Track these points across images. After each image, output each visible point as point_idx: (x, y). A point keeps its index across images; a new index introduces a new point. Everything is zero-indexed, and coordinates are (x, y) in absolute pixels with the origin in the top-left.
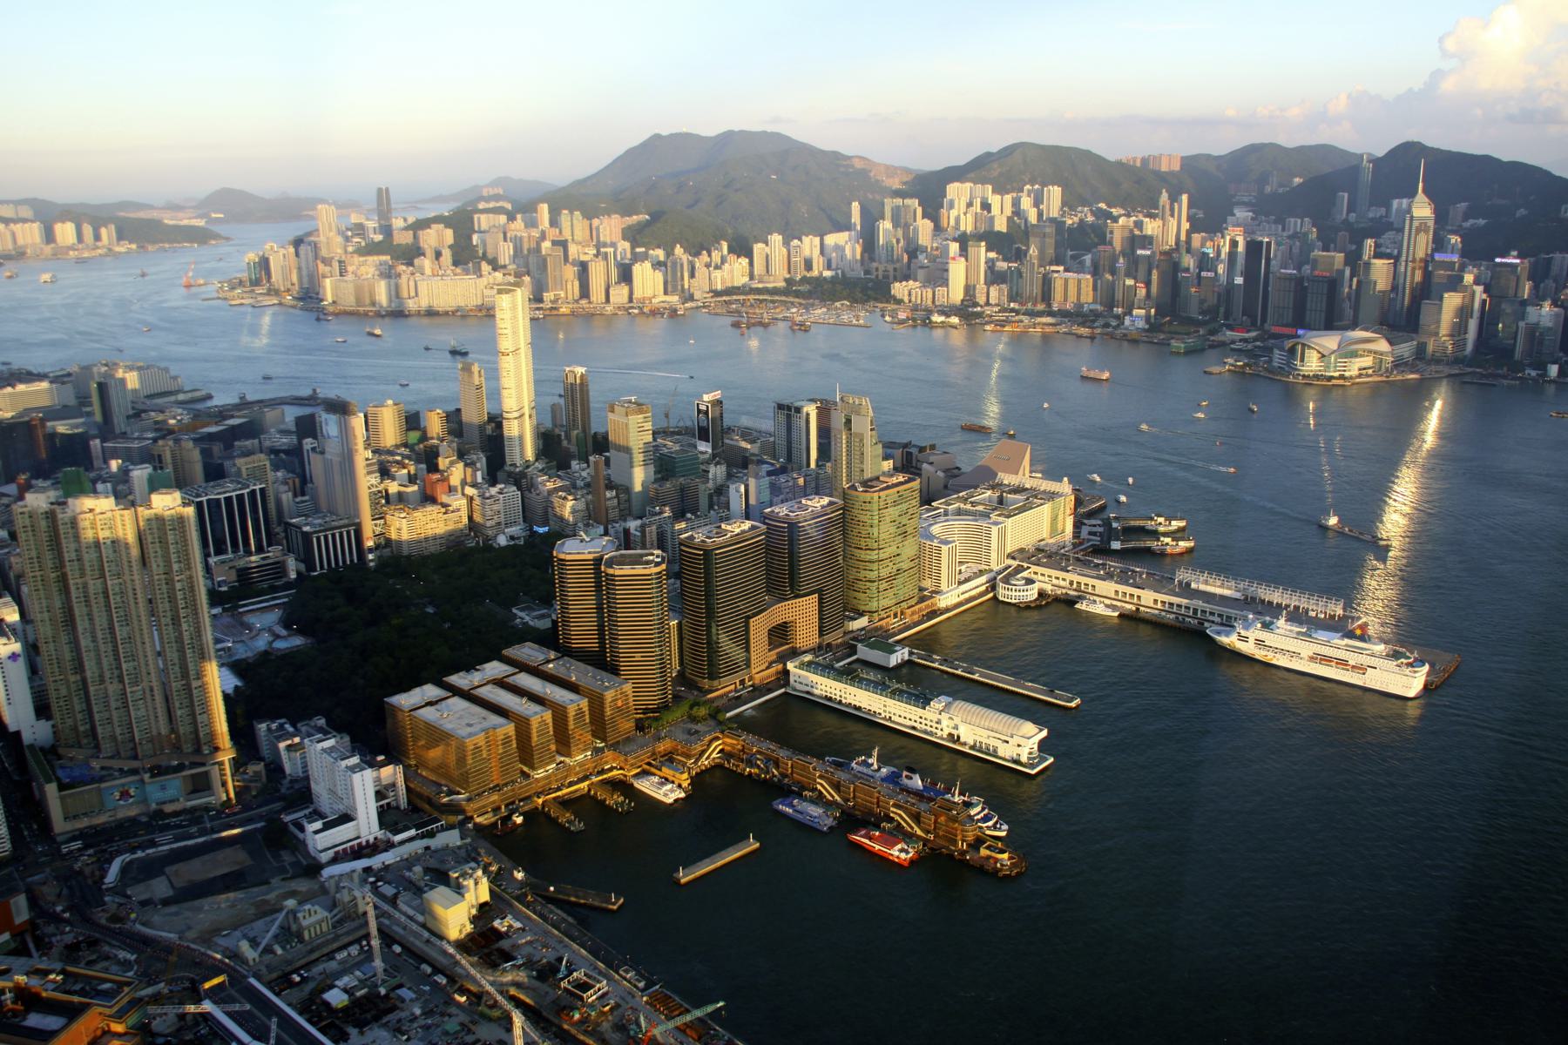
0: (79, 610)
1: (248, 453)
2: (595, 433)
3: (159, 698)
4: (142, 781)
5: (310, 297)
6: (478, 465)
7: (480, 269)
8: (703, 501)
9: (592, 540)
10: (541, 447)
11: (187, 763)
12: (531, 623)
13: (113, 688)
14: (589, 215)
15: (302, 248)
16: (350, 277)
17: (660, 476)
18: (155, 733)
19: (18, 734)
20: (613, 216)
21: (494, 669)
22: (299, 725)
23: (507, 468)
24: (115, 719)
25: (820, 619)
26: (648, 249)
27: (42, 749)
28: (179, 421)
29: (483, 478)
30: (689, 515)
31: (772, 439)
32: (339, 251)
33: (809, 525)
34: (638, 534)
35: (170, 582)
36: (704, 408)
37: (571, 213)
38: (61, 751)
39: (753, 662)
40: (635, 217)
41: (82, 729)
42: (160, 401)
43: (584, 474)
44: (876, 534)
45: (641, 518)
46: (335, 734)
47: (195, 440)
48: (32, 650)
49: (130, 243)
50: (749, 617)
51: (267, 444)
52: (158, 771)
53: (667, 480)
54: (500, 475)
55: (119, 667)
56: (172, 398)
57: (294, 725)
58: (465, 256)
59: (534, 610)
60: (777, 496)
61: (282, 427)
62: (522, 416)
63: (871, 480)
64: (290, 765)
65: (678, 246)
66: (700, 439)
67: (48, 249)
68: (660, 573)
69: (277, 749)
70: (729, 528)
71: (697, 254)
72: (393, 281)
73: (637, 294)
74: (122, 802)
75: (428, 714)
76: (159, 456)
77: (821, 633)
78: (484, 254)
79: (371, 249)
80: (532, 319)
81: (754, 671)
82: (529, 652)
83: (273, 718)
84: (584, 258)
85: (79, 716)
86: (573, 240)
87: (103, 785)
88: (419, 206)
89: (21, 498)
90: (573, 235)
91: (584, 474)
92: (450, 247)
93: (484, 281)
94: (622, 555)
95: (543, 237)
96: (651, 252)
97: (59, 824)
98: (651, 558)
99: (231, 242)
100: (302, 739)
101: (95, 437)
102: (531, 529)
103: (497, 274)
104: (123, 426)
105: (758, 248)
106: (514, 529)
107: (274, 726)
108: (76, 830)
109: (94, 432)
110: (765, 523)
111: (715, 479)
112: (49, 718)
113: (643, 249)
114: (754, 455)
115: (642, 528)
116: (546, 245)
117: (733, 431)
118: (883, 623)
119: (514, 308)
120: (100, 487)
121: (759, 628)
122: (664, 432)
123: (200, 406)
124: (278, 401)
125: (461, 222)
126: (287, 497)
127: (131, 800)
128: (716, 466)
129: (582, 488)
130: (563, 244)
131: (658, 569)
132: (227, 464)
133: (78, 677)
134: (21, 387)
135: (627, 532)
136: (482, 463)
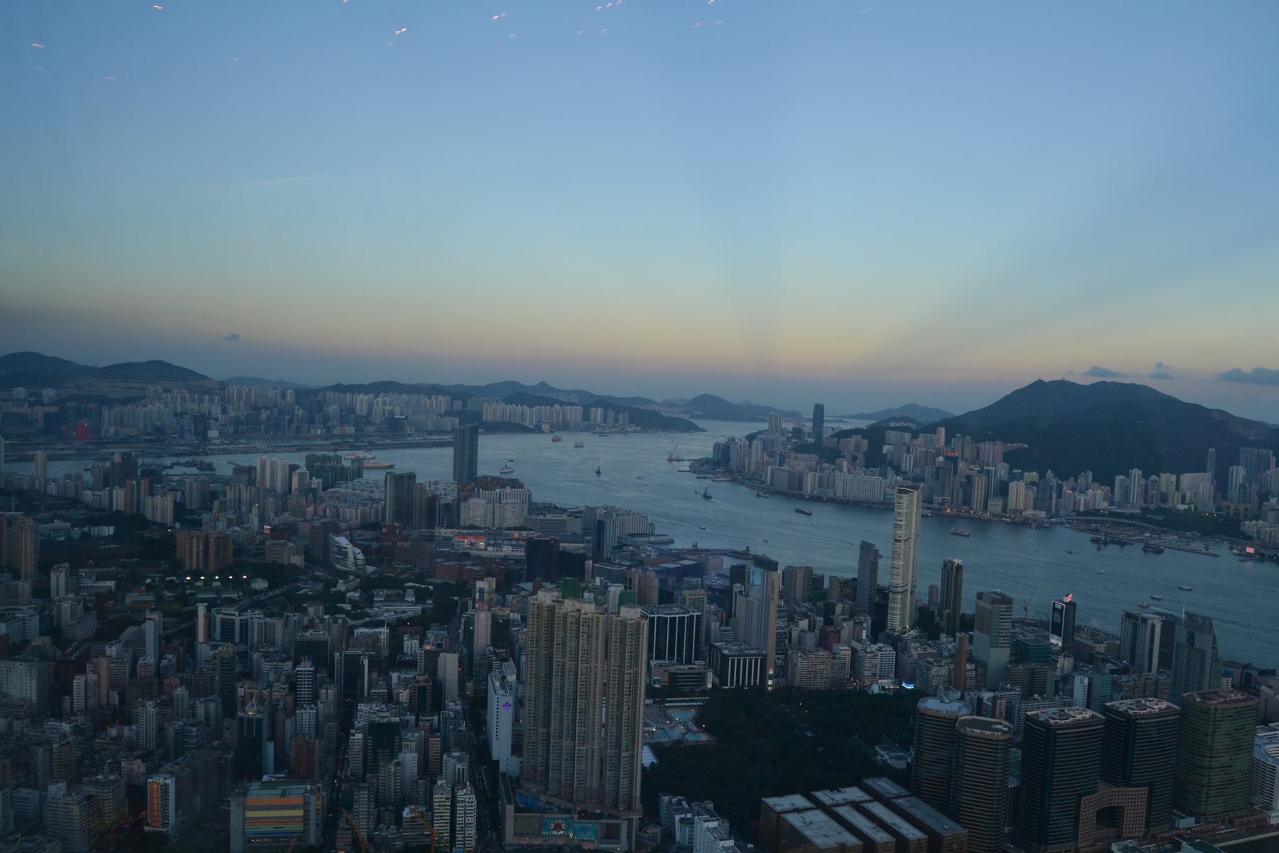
0: (556, 681)
1: (694, 587)
2: (963, 614)
3: (596, 759)
4: (572, 818)
5: (755, 479)
6: (865, 625)
7: (885, 474)
8: (1050, 687)
9: (951, 702)
10: (917, 618)
11: (606, 814)
12: (889, 762)
13: (566, 743)
14: (978, 438)
15: (755, 443)
16: (786, 467)
17: (1013, 658)
18: (588, 785)
19: (498, 762)
20: (997, 442)
21: (854, 793)
22: (693, 804)
23: (887, 631)
24: (563, 769)
25: (1149, 810)
26: (1024, 471)
27: (510, 777)
28: (650, 555)
29: (867, 636)
30: (1036, 696)
31: (1118, 642)
32: (781, 447)
33: (1146, 723)
34: (990, 704)
35: (621, 673)
36: (1059, 606)
37: (963, 436)
38: (522, 782)
39: (1080, 837)
40: (1015, 444)
41: (539, 769)
42: (636, 539)
43: (950, 646)
44: (1209, 744)
45: (994, 691)
46: (718, 817)
47: (657, 572)
48: (519, 703)
50: (1080, 796)
51: (707, 582)
52: (585, 815)
53: (1020, 663)
54: (881, 636)
55: (574, 730)
56: (646, 539)
57: (689, 804)
58: (875, 460)
59: (894, 751)
60: (1118, 693)
61: (721, 572)
62: (906, 591)
63: (1209, 693)
64: (680, 834)
65: (1050, 471)
66: (1053, 632)
68: (1006, 740)
69: (674, 819)
70: (1071, 713)
71: (1067, 479)
72: (818, 474)
73: (1011, 505)
74: (554, 832)
75: (794, 819)
76: (630, 579)
77: (1148, 823)
78: (891, 461)
79: (802, 448)
80: (923, 516)
81: (1079, 845)
82: (885, 785)
83: (675, 795)
84: (970, 473)
85: (540, 759)
86: (962, 457)
87: (545, 816)
88: (844, 419)
89: (534, 592)
90: (962, 454)
91: (950, 646)
92: (864, 453)
93: (888, 481)
94: (974, 719)
95: (938, 454)
96: (1026, 474)
97: (510, 837)
98: (999, 726)
99: (705, 433)
100: (693, 816)
101: (590, 558)
102: (900, 684)
103: (898, 478)
104: (609, 553)
105: (1119, 478)
106: (886, 681)
107: (674, 800)
108: (520, 845)
109: (589, 554)
110: (1104, 714)
111: (1062, 669)
112: (520, 756)
113: (1019, 471)
114: (1100, 653)
115: (994, 699)
116: (941, 459)
117: (1083, 630)
118: (1211, 826)
119: (911, 504)
120: (586, 595)
121: (1089, 808)
122: (1021, 622)
123: (664, 547)
124: (720, 552)
125: (875, 435)
126: (715, 625)
127: (562, 832)
128: (1064, 657)
129: (946, 658)
130: (954, 460)
131: (1005, 737)
132: (676, 593)
133: (545, 731)
134: (549, 516)
135: (980, 700)
136: (867, 623)
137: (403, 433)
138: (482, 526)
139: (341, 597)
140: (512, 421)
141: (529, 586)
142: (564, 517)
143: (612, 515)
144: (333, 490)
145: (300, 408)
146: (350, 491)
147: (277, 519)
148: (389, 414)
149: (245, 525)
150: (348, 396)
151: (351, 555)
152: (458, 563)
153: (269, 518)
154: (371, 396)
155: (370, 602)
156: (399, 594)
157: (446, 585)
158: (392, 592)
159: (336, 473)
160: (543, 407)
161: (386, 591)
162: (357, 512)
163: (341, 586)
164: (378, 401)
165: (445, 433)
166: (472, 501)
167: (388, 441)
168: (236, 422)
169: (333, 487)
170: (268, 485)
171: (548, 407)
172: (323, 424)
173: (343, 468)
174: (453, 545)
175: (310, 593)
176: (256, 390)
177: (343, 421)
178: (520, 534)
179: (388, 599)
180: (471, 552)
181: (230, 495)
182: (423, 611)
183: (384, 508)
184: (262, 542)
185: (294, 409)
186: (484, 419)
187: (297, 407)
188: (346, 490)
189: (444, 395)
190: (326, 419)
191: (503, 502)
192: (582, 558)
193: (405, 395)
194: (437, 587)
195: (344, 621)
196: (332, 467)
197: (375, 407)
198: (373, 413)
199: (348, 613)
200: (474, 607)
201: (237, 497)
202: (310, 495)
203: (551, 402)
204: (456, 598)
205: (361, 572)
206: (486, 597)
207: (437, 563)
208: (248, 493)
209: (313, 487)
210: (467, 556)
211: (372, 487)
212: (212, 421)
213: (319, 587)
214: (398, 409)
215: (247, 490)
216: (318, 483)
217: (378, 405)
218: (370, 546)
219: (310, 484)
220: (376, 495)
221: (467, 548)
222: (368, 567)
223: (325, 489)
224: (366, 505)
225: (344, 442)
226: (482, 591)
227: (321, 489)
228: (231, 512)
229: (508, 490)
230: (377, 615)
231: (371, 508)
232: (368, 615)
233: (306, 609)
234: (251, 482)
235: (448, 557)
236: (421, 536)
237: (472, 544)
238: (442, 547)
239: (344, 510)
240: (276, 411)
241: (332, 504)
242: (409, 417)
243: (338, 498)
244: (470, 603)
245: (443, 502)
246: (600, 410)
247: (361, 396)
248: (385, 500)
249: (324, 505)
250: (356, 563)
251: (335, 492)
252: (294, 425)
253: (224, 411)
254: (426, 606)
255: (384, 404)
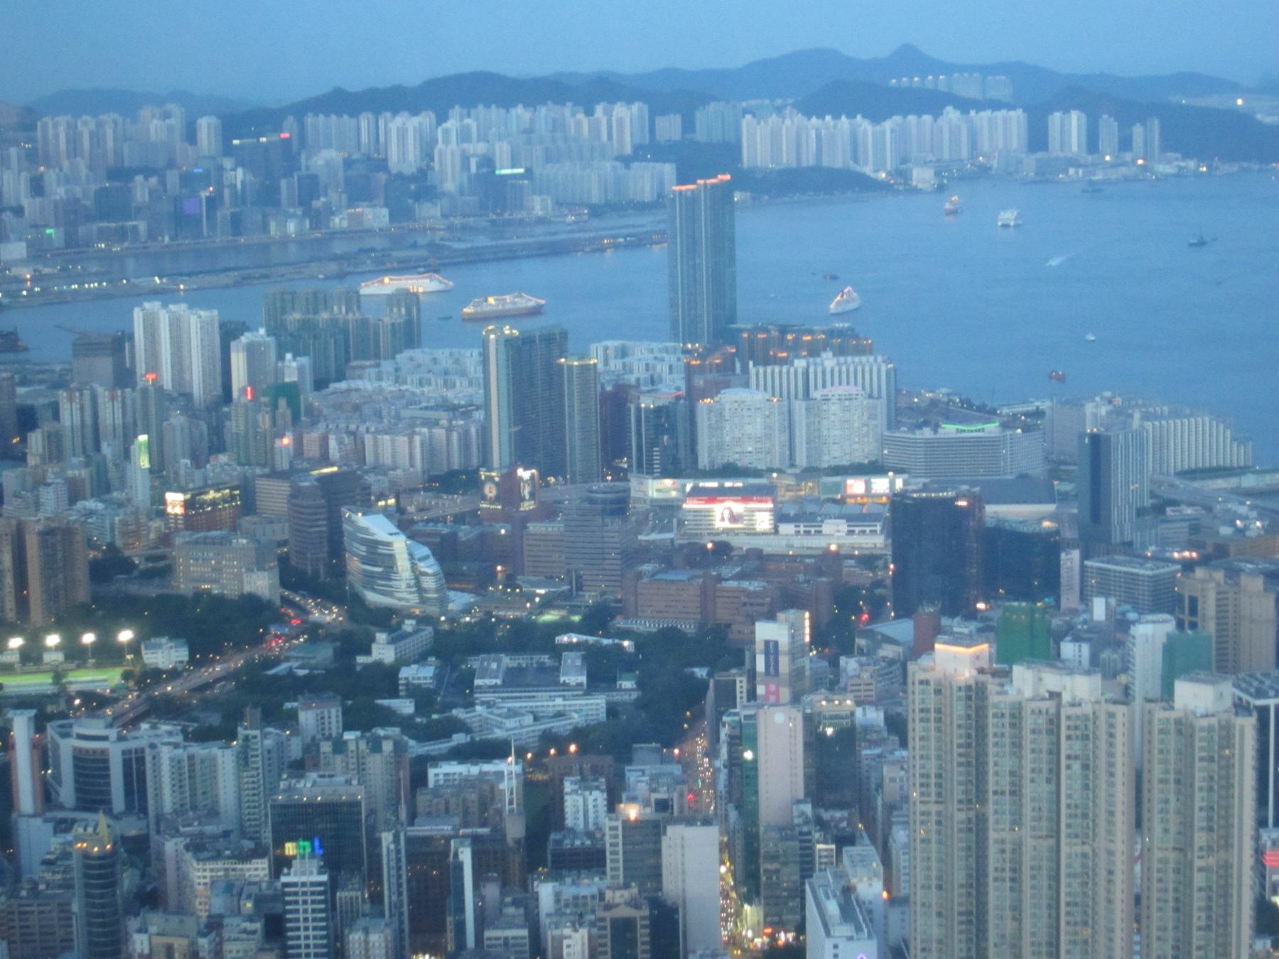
49: (1186, 156)
67: (1030, 163)
101: (1070, 545)
109: (1069, 534)
134: (949, 429)
137: (524, 214)
138: (761, 466)
139: (386, 679)
140: (825, 163)
141: (903, 629)
142: (992, 428)
143: (1131, 416)
144: (343, 385)
145: (240, 163)
146: (388, 386)
147: (198, 474)
148: (479, 166)
149: (115, 494)
150: (364, 124)
151: (403, 563)
152: (699, 572)
153: (176, 473)
154: (425, 119)
155: (463, 689)
156: (542, 668)
157: (670, 637)
158: (523, 661)
159: (346, 341)
160: (912, 118)
161: (507, 661)
162: (411, 442)
163: (383, 651)
164: (446, 133)
165: (642, 207)
166: (729, 397)
167: (482, 241)
168: (71, 214)
169: (341, 377)
170: (167, 383)
171: (927, 118)
172: (301, 203)
173: (364, 323)
174: (681, 523)
175: (301, 672)
176: (115, 122)
177: (358, 192)
178: (868, 486)
179: (514, 680)
180: (735, 541)
181: (70, 415)
182: (612, 710)
183: (485, 432)
184: (165, 539)
185: (220, 169)
186: (746, 162)
187: (228, 163)
188: (376, 384)
189: (630, 101)
190: (310, 188)
191: (817, 394)
192: (1049, 547)
193: (519, 110)
194: (643, 642)
195: (399, 747)
196: (334, 322)
197: (440, 145)
198: (436, 165)
199: (406, 724)
200: (752, 695)
201: (88, 421)
202: (282, 402)
203: (932, 103)
204: (701, 672)
205: (433, 610)
206: (784, 664)
207: (640, 576)
208: (118, 405)
209: (287, 380)
210: (723, 549)
211: (446, 372)
212: (7, 216)
213: (325, 653)
214: (502, 150)
215: (113, 399)
216: (301, 370)
217: (447, 141)
218: (454, 535)
219: (279, 373)
220: (460, 393)
221: (727, 531)
222: (452, 594)
223: (320, 384)
224: (435, 423)
225: (362, 251)
226: (771, 649)
227: (308, 385)
228: (75, 460)
229: (829, 360)
230: (486, 725)
231: (449, 429)
232: (463, 727)
233: (293, 715)
234: (124, 377)
235: (668, 557)
236: (591, 501)
237: (734, 518)
238: (653, 530)
239: (376, 445)
240: (172, 178)
241: (343, 426)
242: (537, 171)
243: (357, 408)
244: (741, 684)
245: (647, 403)
246: (1075, 117)
247: (399, 120)
248: (486, 406)
249: (321, 427)
250: (418, 583)
251: (349, 391)
252: (224, 213)
253: (37, 187)
254: (617, 697)
255: (464, 136)
